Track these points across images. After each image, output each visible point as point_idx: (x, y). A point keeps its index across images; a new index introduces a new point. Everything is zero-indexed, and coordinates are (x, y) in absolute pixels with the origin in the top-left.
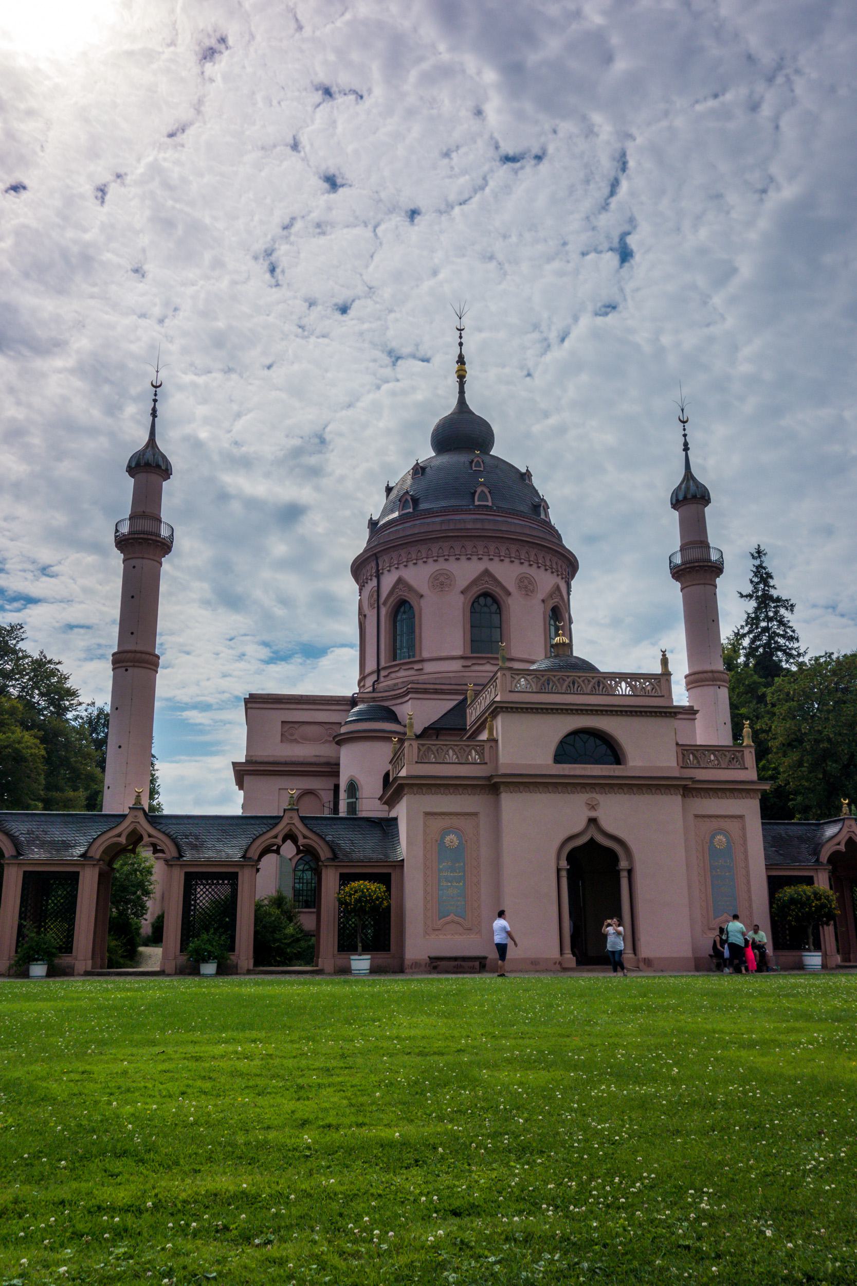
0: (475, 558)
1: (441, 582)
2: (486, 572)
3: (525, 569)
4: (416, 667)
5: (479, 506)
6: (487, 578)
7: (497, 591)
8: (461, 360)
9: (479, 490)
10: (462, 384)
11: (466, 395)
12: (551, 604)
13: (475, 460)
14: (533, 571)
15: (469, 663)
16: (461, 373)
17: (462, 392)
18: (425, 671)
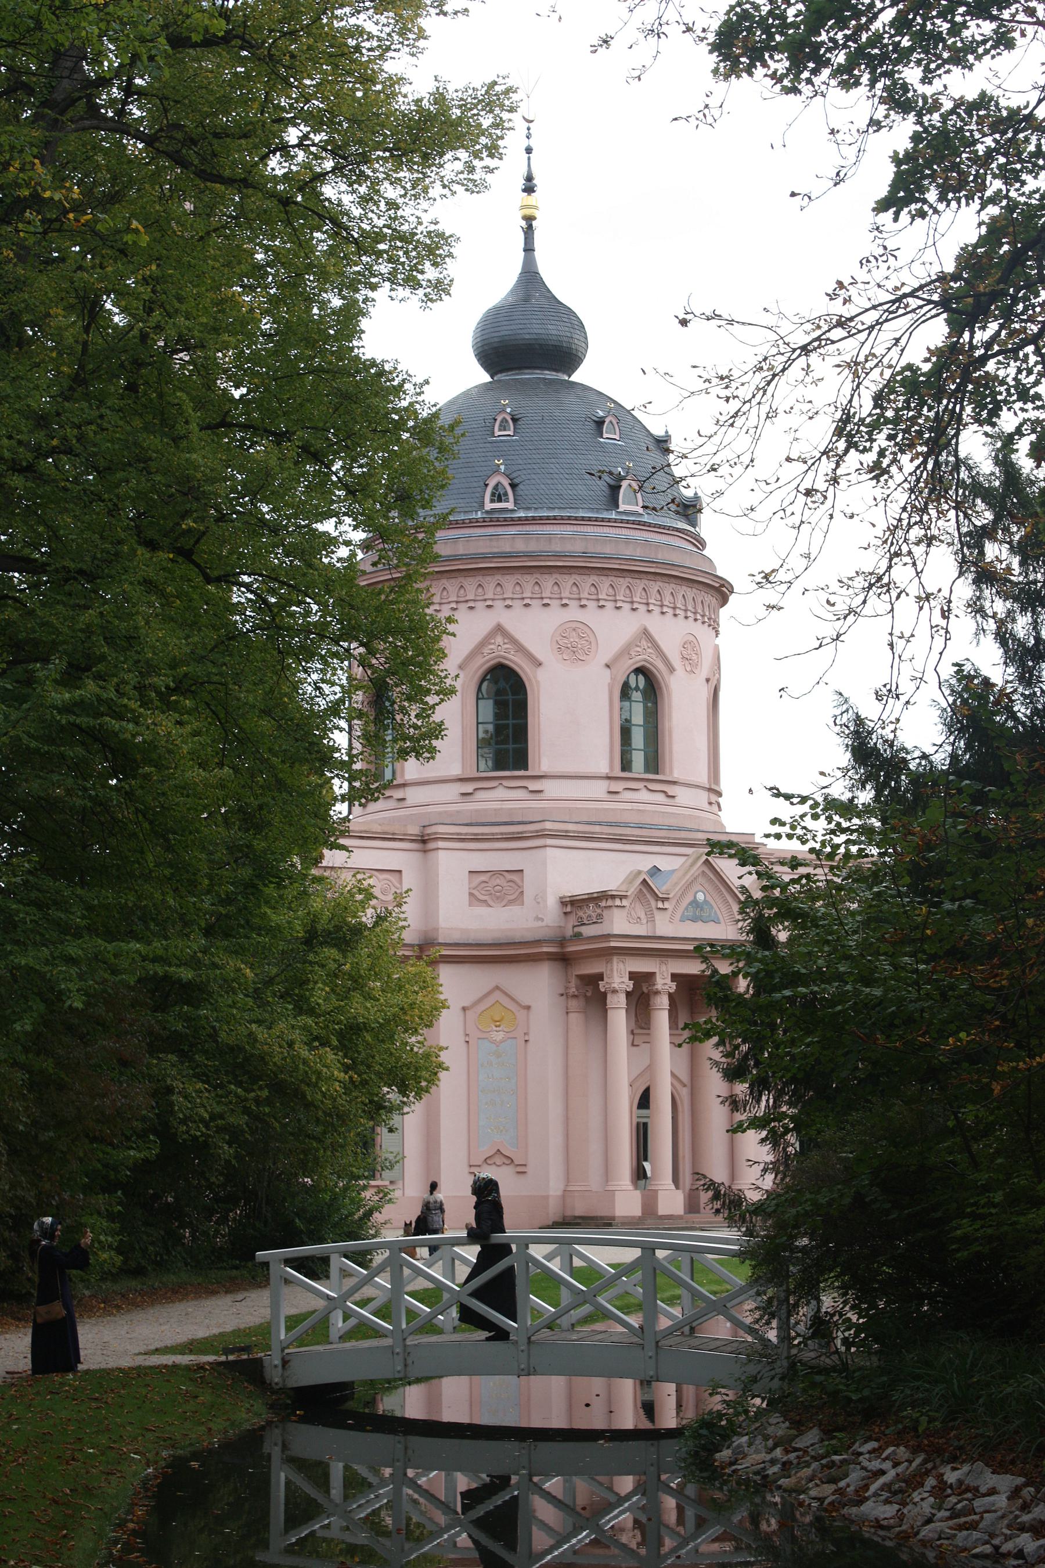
0: (480, 605)
2: (499, 629)
3: (573, 613)
4: (398, 794)
5: (493, 511)
6: (499, 640)
8: (529, 189)
9: (492, 483)
10: (529, 232)
11: (538, 254)
13: (499, 419)
14: (591, 616)
15: (469, 788)
16: (528, 212)
17: (529, 249)
18: (409, 802)
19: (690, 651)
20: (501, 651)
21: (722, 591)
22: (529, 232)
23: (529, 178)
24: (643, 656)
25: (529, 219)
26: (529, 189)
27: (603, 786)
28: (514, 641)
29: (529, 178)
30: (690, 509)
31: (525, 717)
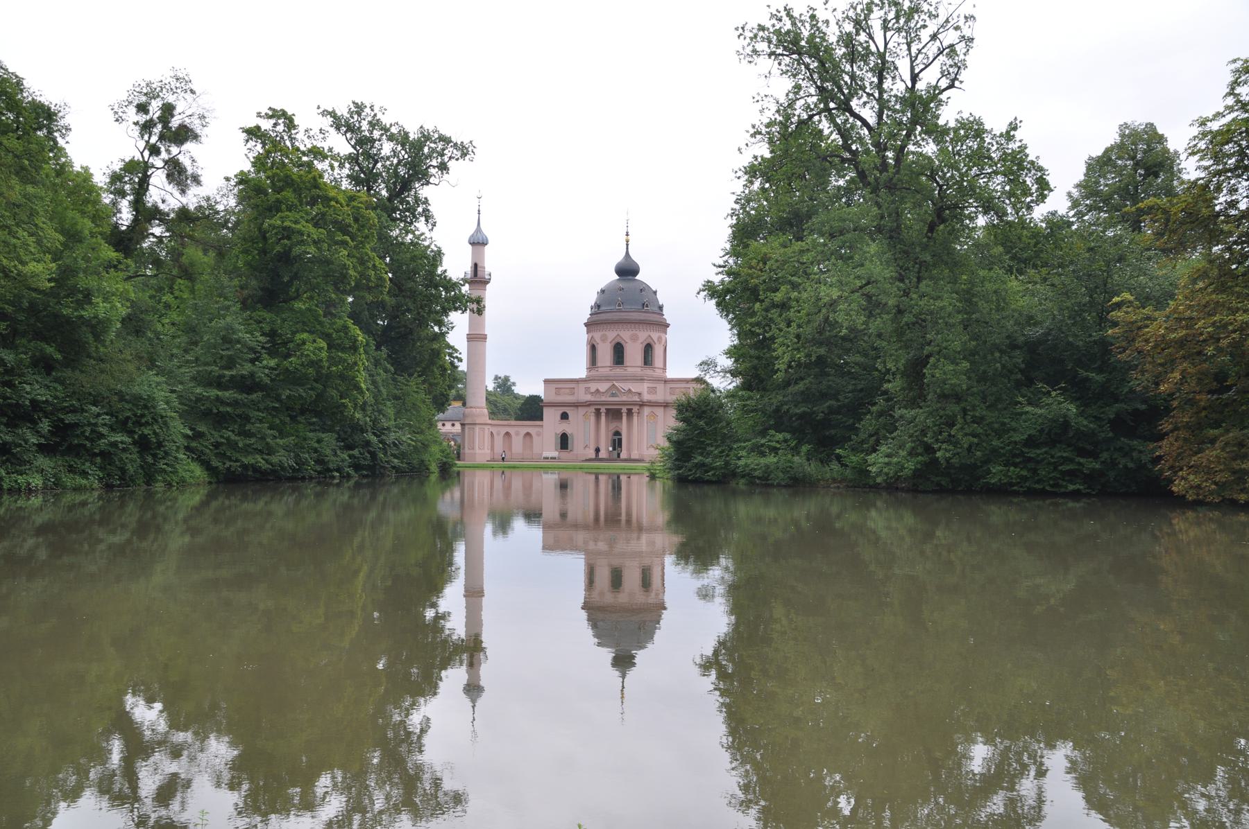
1: (604, 339)
3: (634, 332)
7: (622, 342)
8: (627, 235)
10: (627, 245)
12: (646, 343)
17: (627, 248)
19: (660, 339)
20: (620, 341)
21: (668, 326)
22: (627, 245)
23: (627, 233)
24: (649, 341)
25: (627, 241)
26: (627, 235)
27: (639, 369)
28: (621, 337)
29: (627, 233)
30: (661, 308)
31: (623, 353)
